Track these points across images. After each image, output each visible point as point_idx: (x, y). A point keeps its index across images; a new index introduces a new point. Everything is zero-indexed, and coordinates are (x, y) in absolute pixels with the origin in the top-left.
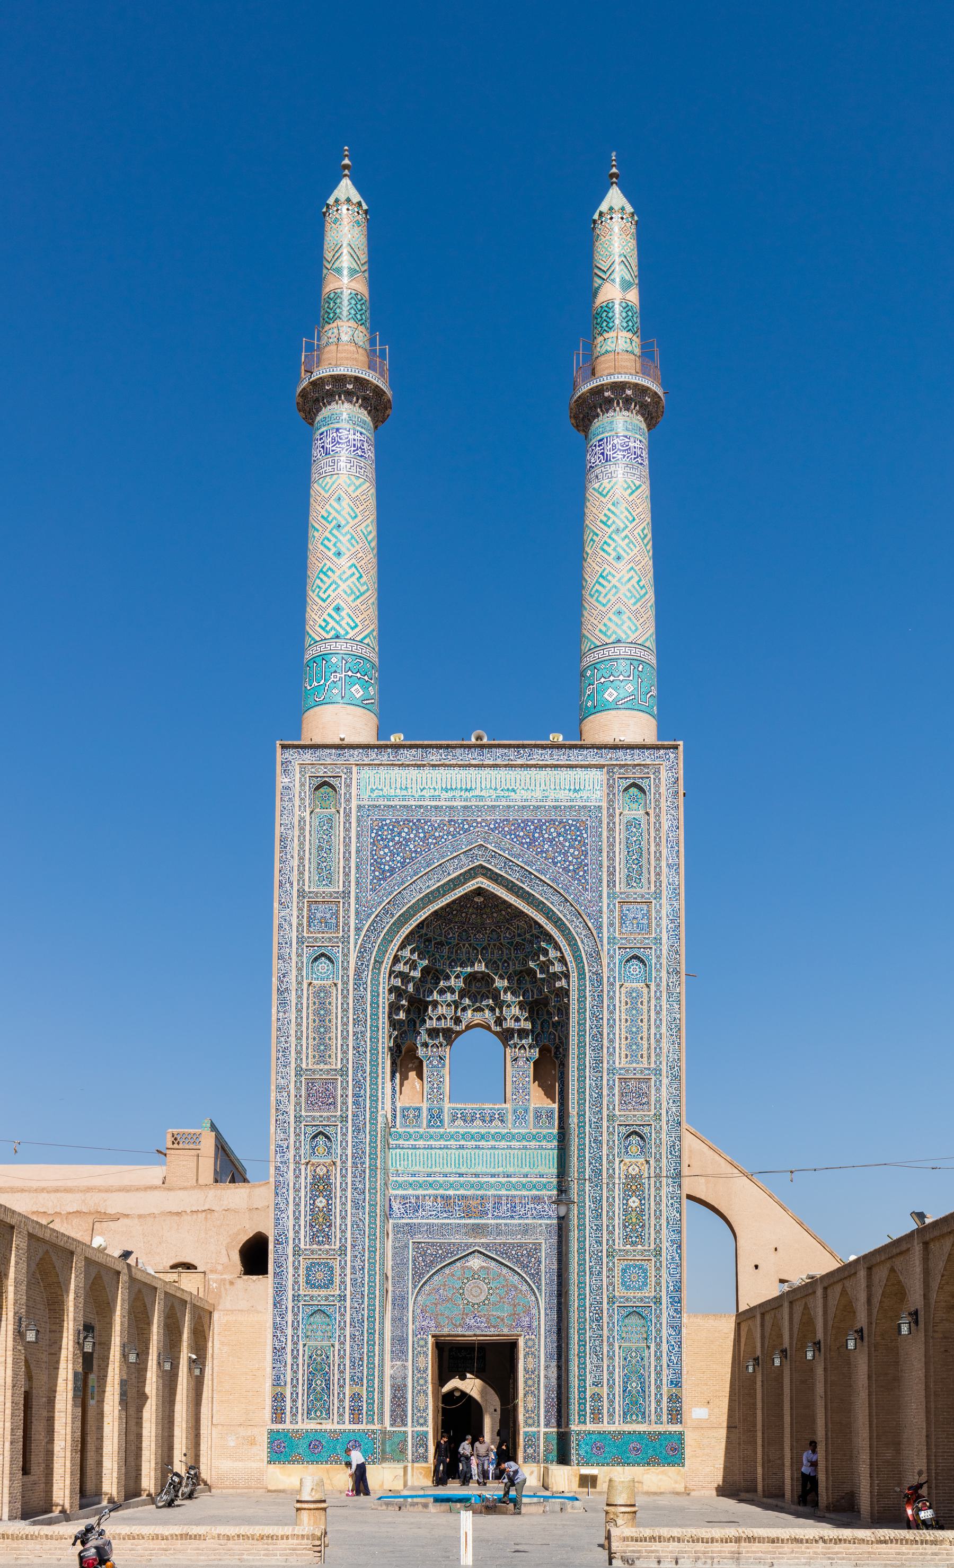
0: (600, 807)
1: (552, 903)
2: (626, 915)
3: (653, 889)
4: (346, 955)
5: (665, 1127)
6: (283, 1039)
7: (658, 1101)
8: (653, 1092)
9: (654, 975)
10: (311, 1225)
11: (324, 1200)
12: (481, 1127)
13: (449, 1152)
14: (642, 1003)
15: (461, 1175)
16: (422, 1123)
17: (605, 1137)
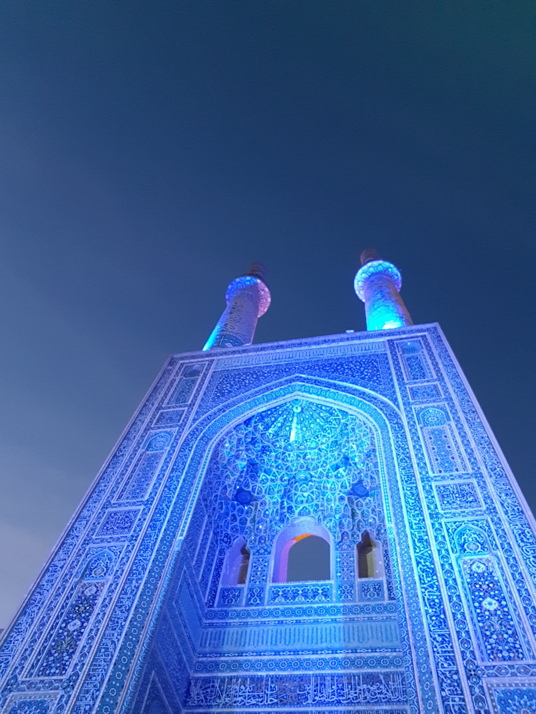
0: (386, 354)
1: (354, 394)
2: (417, 392)
3: (435, 377)
4: (179, 433)
5: (503, 517)
6: (103, 485)
7: (487, 498)
8: (478, 490)
9: (451, 416)
10: (50, 654)
11: (79, 623)
12: (303, 603)
13: (266, 629)
14: (445, 436)
15: (277, 653)
16: (241, 601)
17: (431, 533)
